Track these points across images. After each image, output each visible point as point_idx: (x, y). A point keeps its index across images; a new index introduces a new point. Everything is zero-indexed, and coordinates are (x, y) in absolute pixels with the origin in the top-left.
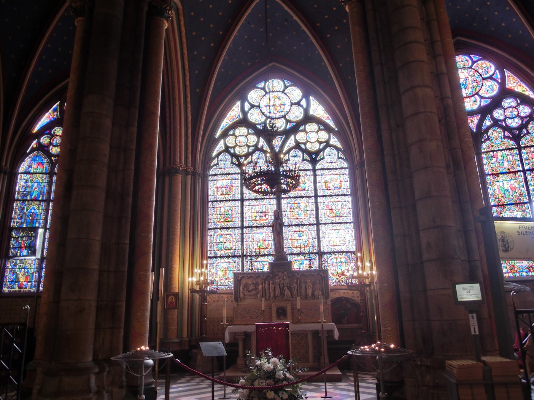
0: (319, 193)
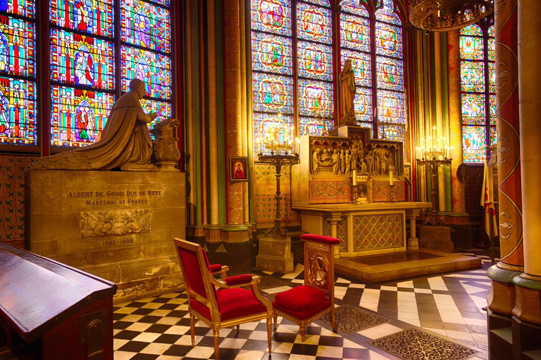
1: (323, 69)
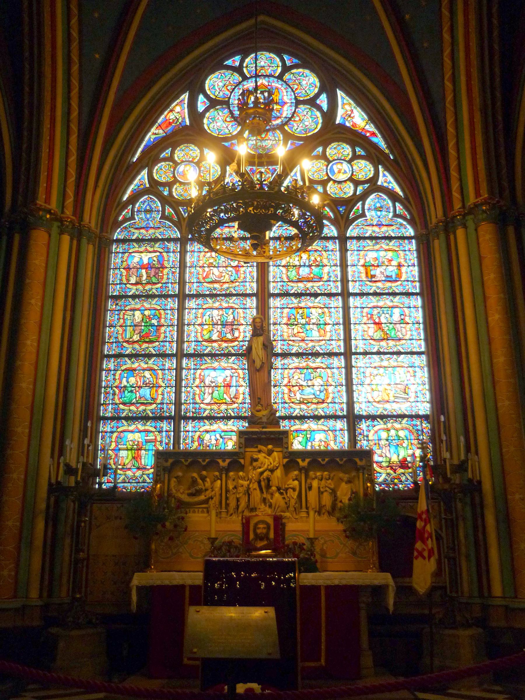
0: (353, 288)
1: (236, 334)
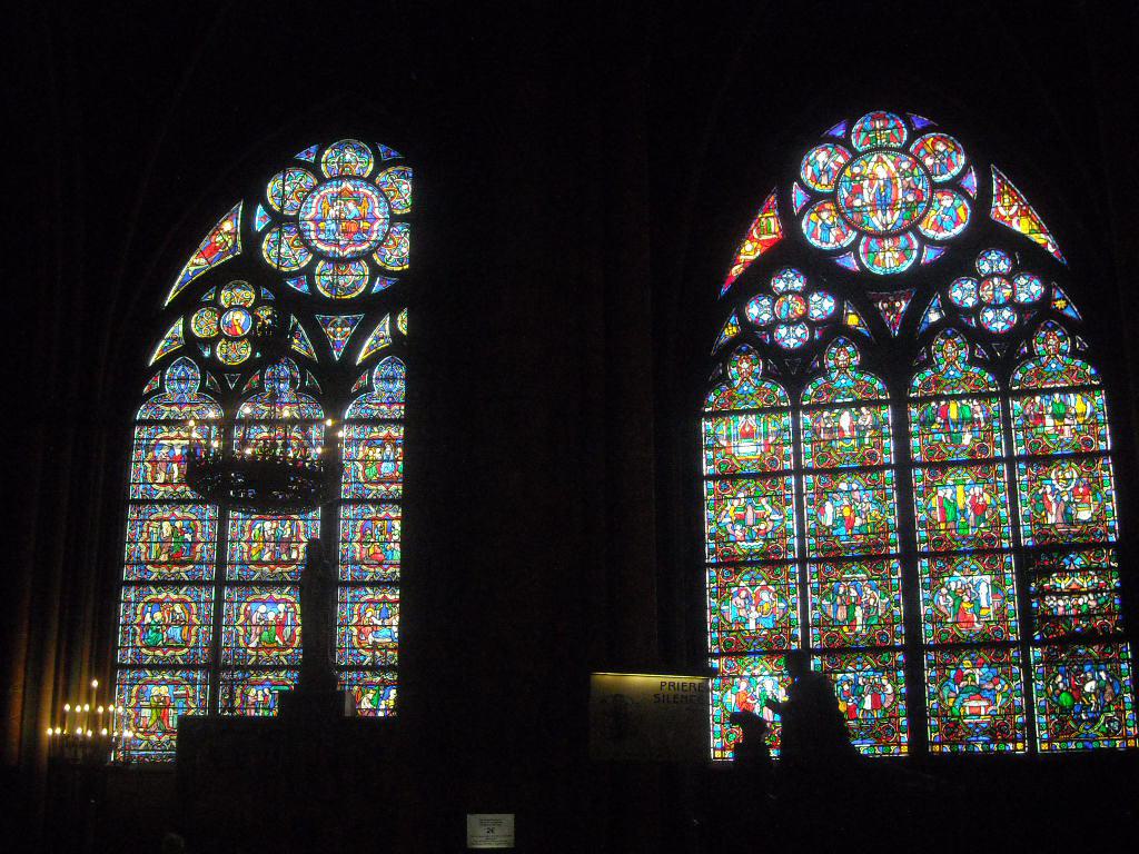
1: (294, 556)
